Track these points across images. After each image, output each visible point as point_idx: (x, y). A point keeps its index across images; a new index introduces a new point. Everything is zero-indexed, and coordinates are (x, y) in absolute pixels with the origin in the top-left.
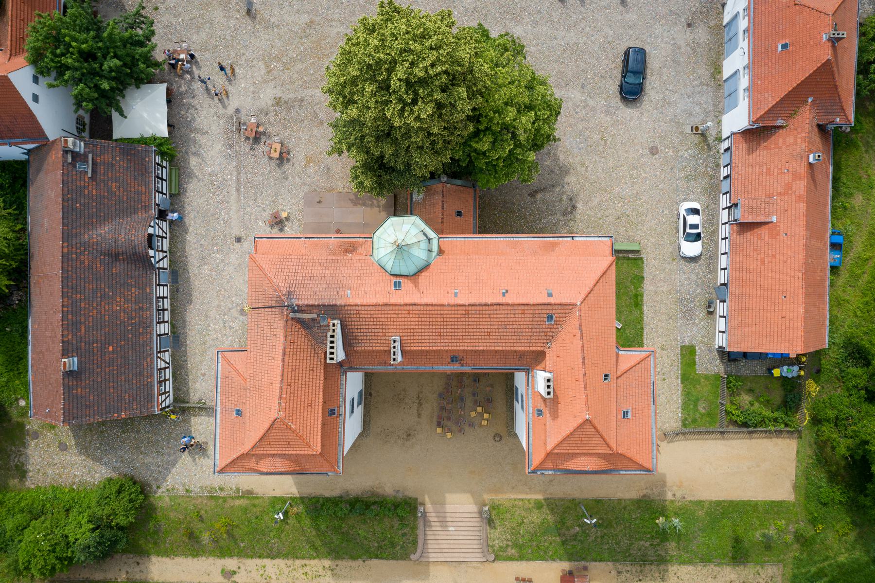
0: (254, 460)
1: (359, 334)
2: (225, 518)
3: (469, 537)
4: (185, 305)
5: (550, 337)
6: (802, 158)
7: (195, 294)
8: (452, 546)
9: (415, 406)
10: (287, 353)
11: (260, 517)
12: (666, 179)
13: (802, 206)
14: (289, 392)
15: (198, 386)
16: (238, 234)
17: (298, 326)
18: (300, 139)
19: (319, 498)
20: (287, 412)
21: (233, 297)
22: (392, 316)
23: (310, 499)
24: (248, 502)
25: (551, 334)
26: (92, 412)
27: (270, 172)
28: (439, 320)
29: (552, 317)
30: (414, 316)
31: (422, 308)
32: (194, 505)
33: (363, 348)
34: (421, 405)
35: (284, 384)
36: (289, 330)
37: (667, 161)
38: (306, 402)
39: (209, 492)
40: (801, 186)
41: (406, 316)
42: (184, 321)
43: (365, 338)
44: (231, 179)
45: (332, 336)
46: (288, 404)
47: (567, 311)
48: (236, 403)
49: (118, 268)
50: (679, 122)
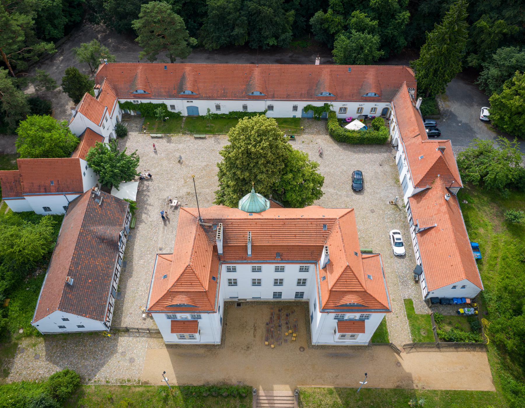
5: (326, 237)
6: (441, 198)
13: (447, 216)
22: (248, 225)
25: (326, 236)
26: (73, 309)
28: (271, 227)
29: (325, 226)
30: (259, 225)
31: (263, 221)
36: (198, 229)
40: (444, 208)
41: (255, 225)
45: (220, 229)
47: (333, 223)
49: (103, 246)
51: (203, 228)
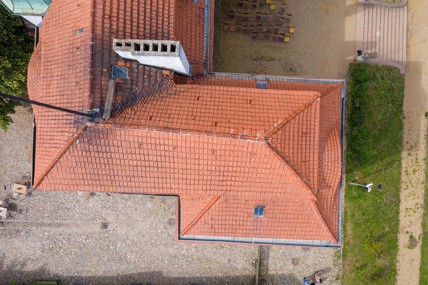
0: (324, 191)
1: (148, 27)
2: (364, 243)
3: (386, 18)
4: (163, 277)
7: (154, 268)
8: (393, 36)
9: (264, 63)
10: (166, 125)
11: (364, 211)
14: (228, 125)
15: (239, 267)
16: (99, 226)
17: (129, 111)
18: (12, 166)
19: (347, 155)
20: (258, 127)
21: (157, 232)
23: (348, 163)
24: (349, 221)
27: (42, 195)
32: (351, 273)
33: (172, 29)
34: (263, 57)
35: (214, 129)
38: (245, 105)
39: (339, 258)
42: (178, 278)
43: (154, 21)
44: (48, 232)
46: (245, 127)
48: (246, 215)
51: (121, 111)
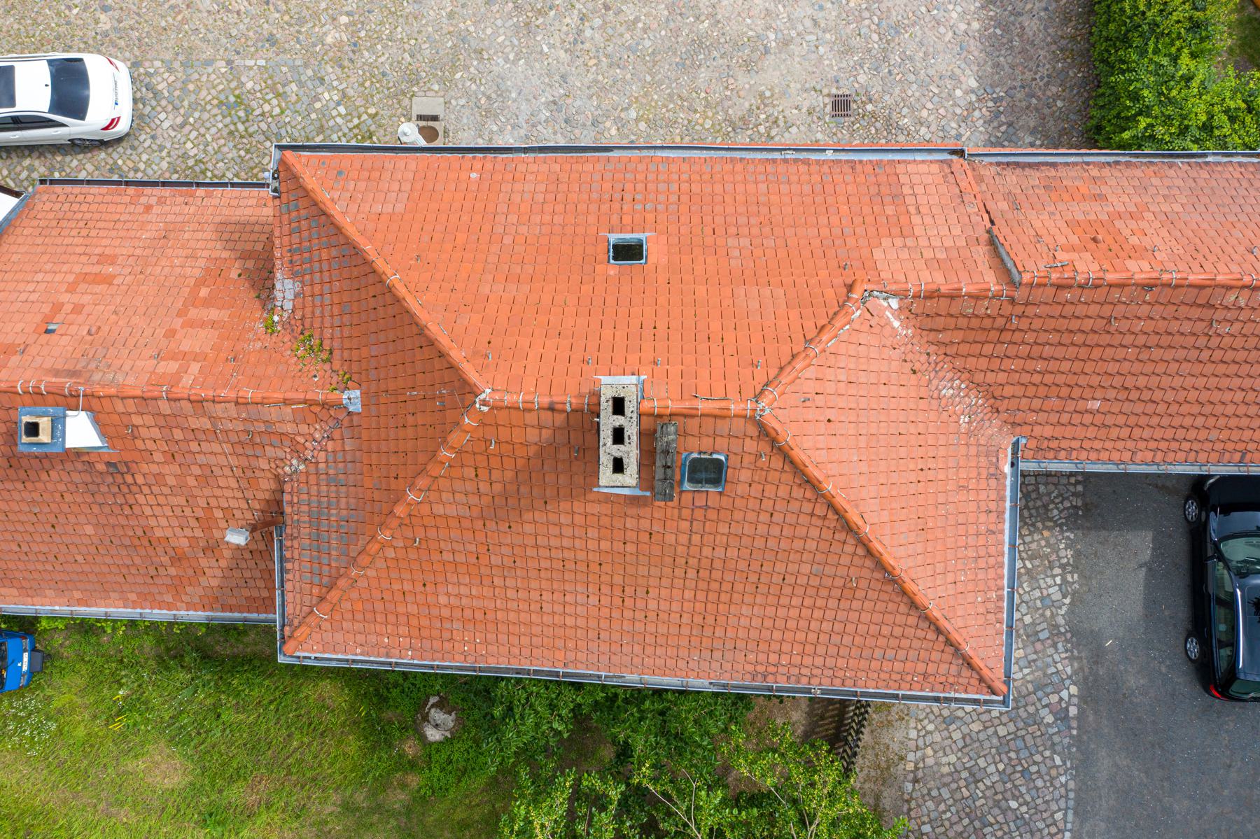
12: (232, 18)
37: (302, 21)
50: (454, 69)
